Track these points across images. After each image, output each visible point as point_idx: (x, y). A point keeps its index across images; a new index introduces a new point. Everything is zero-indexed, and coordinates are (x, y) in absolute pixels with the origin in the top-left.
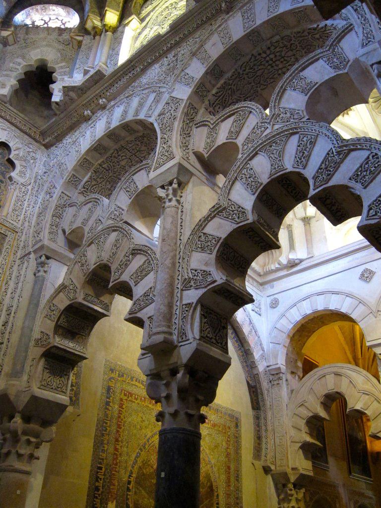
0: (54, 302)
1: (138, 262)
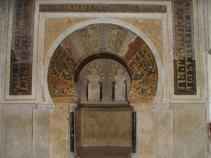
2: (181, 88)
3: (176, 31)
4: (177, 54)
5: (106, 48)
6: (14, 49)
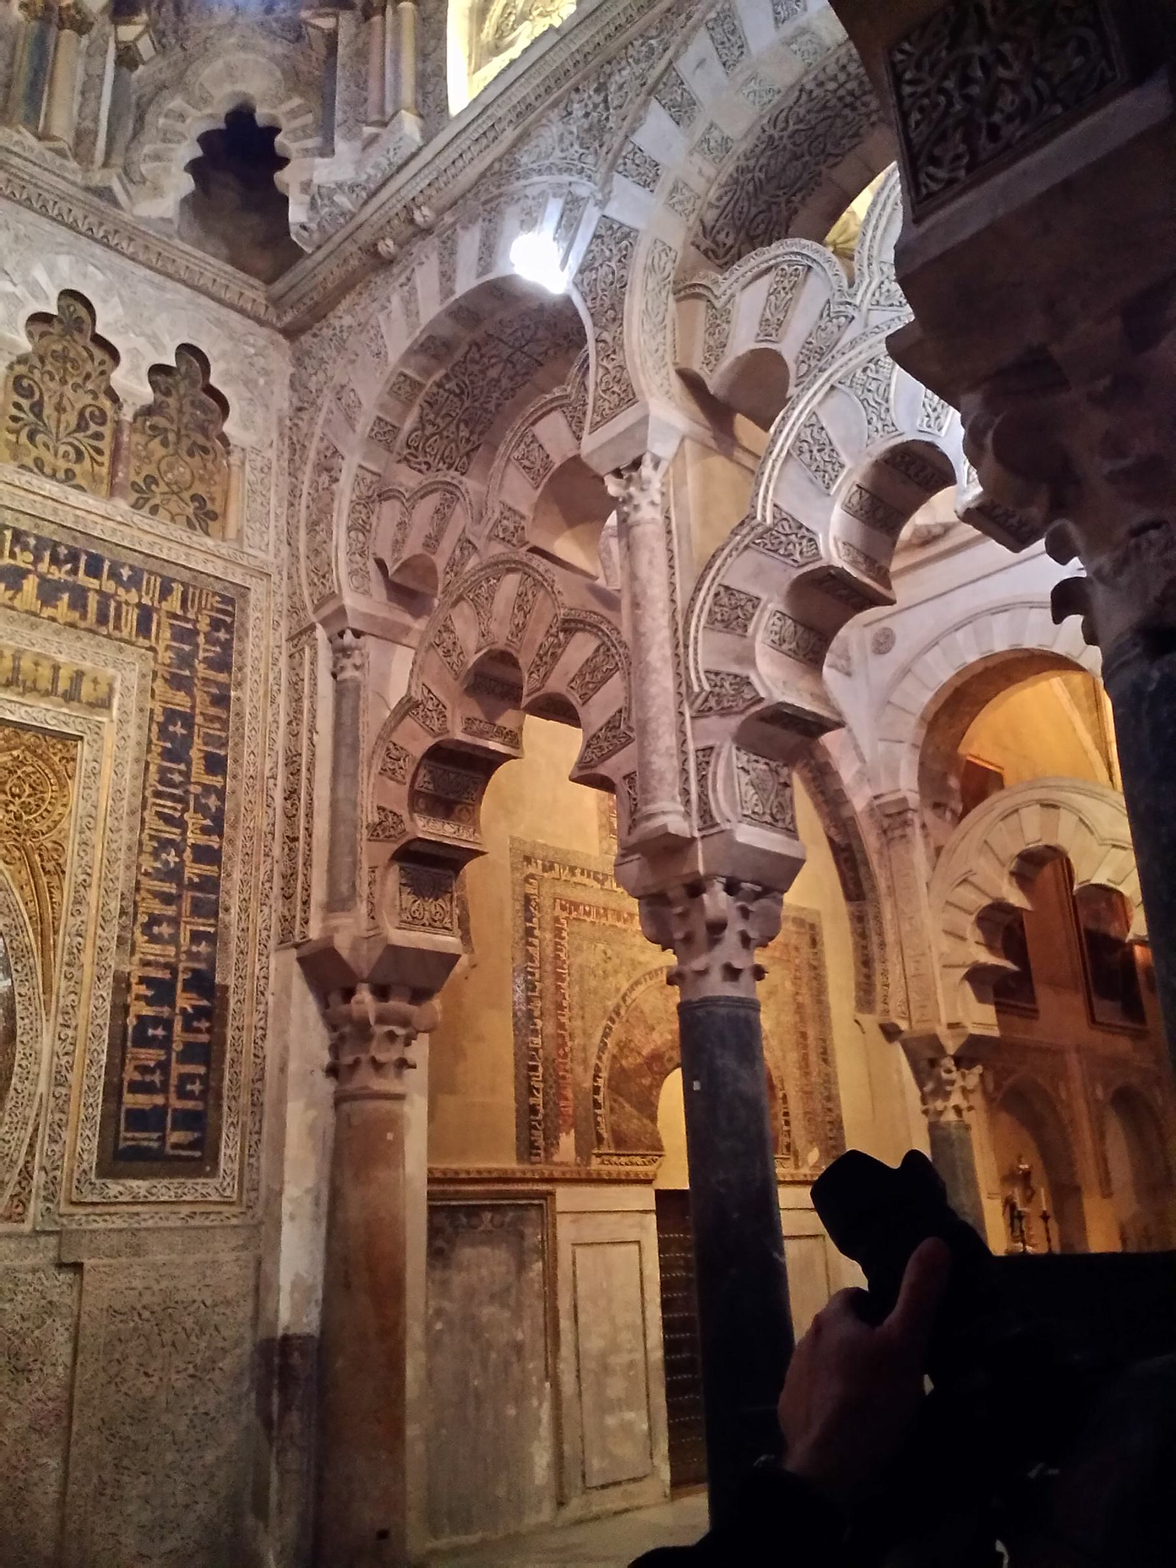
0: (394, 738)
1: (581, 648)
3: (143, 821)
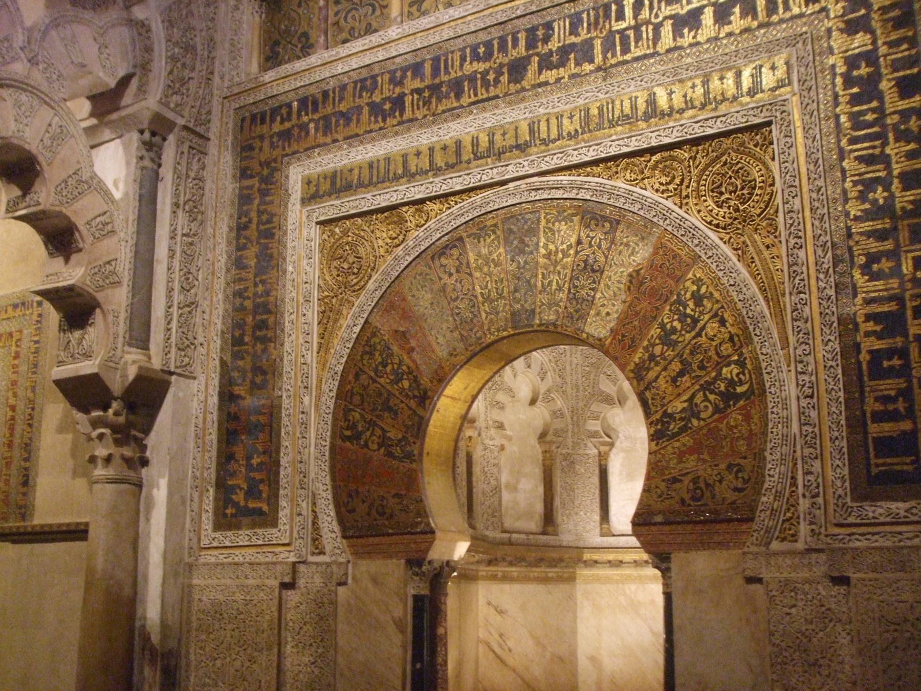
2: (892, 464)
4: (859, 284)
5: (533, 311)
6: (228, 358)
